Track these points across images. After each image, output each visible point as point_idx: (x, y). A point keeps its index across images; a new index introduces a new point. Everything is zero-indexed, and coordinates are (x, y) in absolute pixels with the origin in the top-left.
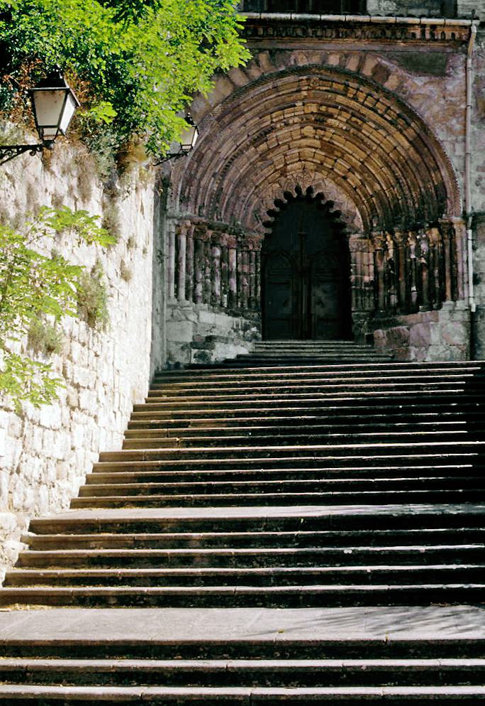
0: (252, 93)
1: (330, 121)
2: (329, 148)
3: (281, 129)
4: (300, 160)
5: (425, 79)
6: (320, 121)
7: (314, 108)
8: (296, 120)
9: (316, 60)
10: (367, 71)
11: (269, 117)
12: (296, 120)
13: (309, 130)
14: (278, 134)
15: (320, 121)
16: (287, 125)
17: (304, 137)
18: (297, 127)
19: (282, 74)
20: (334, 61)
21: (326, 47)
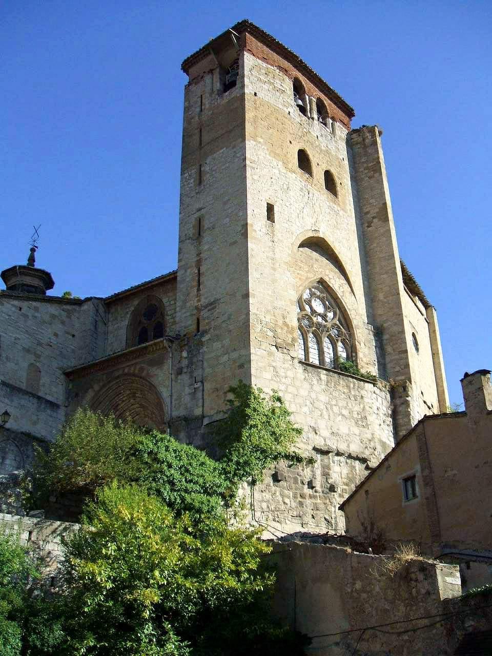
0: (101, 393)
1: (137, 395)
2: (142, 406)
3: (122, 403)
4: (137, 415)
5: (155, 368)
6: (134, 395)
7: (128, 392)
8: (126, 398)
9: (121, 372)
10: (137, 371)
11: (114, 400)
12: (126, 398)
13: (132, 401)
14: (122, 405)
15: (134, 395)
16: (123, 401)
17: (132, 405)
18: (128, 401)
19: (109, 382)
20: (126, 371)
21: (124, 365)
